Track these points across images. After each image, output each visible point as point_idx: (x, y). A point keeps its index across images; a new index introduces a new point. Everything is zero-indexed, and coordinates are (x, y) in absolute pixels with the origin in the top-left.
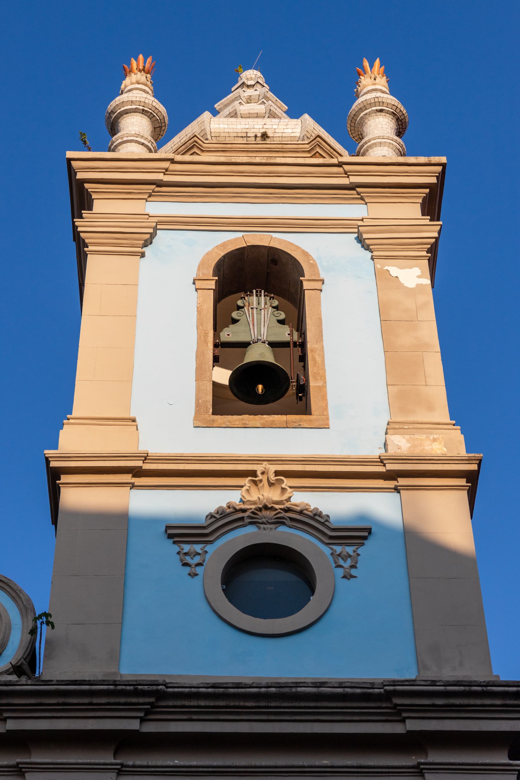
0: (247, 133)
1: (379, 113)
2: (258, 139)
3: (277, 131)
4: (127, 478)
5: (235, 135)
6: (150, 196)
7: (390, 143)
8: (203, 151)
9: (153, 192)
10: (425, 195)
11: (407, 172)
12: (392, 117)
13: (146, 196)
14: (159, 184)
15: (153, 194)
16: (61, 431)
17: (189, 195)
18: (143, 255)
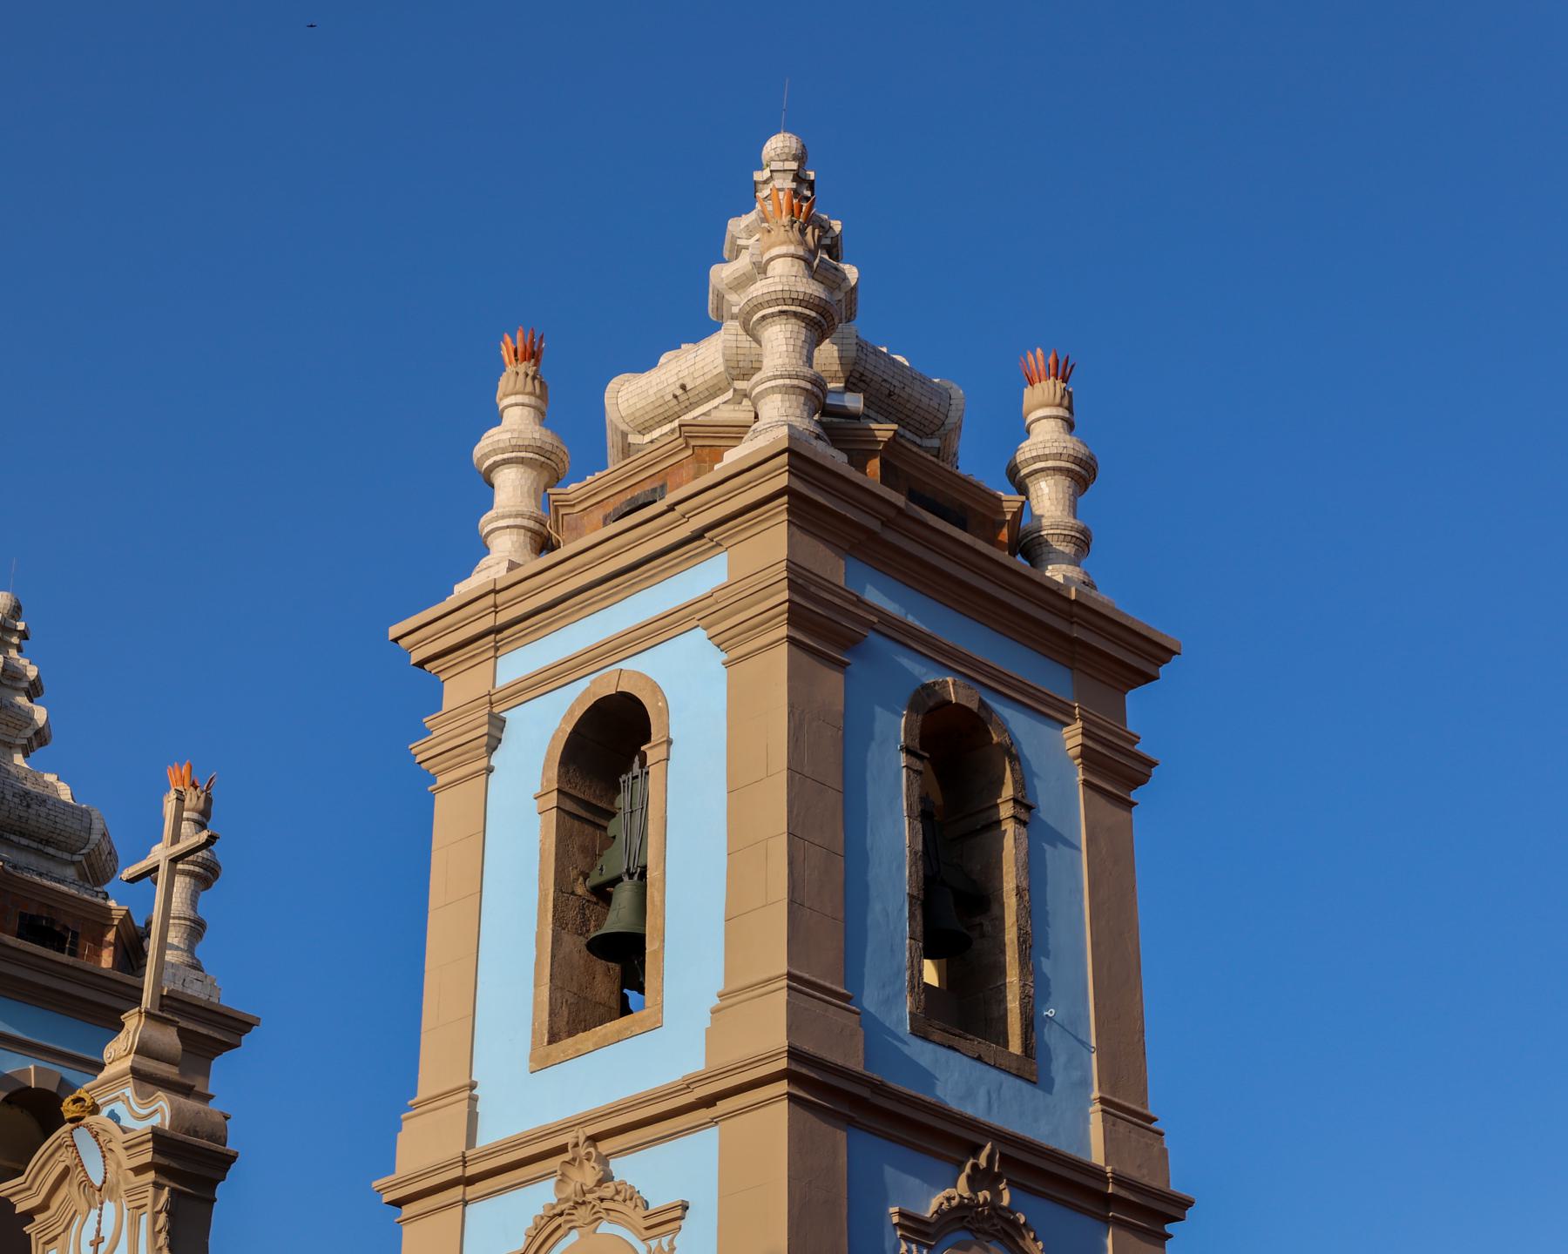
0: (663, 397)
1: (764, 323)
2: (681, 399)
3: (696, 375)
4: (456, 1193)
5: (651, 407)
6: (497, 649)
7: (772, 387)
8: (573, 505)
9: (497, 642)
10: (786, 506)
11: (750, 482)
12: (785, 317)
13: (491, 653)
14: (497, 630)
15: (498, 645)
16: (399, 1134)
17: (535, 630)
18: (490, 770)
